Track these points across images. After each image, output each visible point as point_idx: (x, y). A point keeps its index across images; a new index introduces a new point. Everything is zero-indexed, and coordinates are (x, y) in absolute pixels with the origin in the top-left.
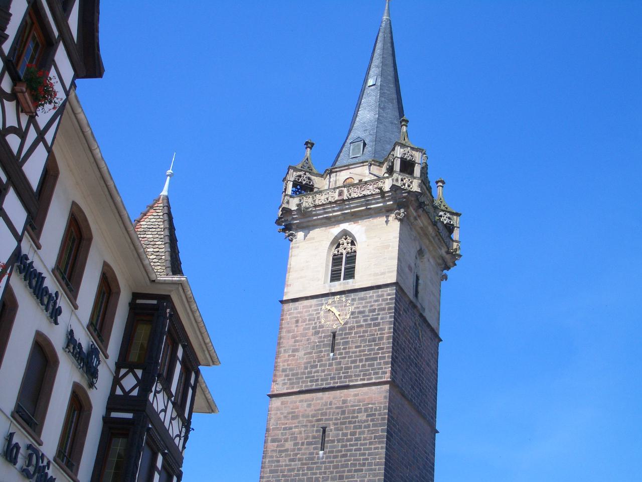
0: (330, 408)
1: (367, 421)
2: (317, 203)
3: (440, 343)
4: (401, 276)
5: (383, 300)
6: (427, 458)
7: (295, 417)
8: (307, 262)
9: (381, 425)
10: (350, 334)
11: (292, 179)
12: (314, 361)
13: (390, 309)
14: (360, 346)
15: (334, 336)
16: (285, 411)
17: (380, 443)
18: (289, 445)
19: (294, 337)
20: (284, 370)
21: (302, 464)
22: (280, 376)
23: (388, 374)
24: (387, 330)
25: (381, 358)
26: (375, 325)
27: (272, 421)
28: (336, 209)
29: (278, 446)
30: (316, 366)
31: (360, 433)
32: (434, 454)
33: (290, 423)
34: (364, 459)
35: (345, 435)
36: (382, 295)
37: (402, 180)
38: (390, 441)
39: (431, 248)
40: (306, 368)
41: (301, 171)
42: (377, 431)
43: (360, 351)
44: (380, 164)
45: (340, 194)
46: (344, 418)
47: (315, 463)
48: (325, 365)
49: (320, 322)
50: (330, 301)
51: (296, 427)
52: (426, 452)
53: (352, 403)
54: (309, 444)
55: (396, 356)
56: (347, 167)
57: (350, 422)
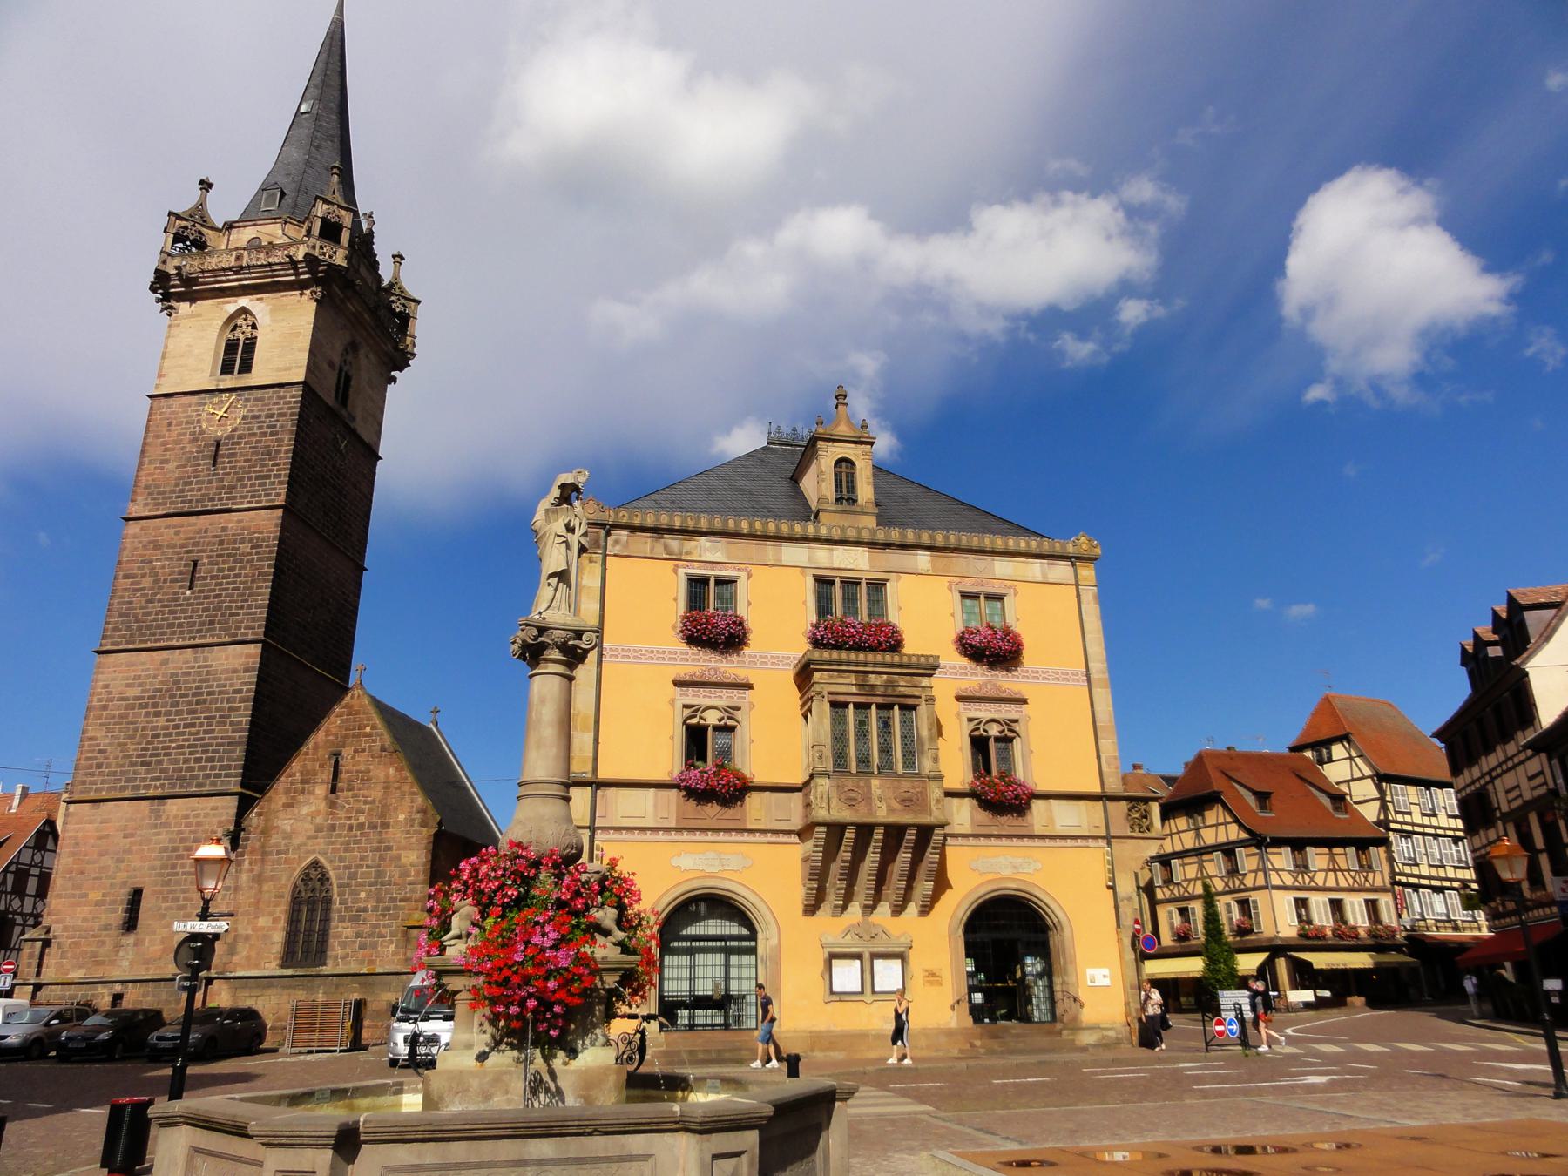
0: (205, 537)
1: (251, 554)
2: (206, 267)
3: (379, 462)
4: (313, 373)
5: (285, 403)
8: (190, 346)
9: (268, 559)
10: (239, 443)
11: (174, 231)
12: (189, 477)
13: (292, 414)
14: (250, 460)
15: (218, 445)
16: (145, 540)
17: (265, 581)
18: (147, 583)
19: (163, 444)
20: (147, 487)
21: (163, 606)
22: (142, 494)
23: (283, 497)
24: (287, 442)
26: (272, 434)
28: (231, 277)
29: (132, 584)
30: (191, 483)
31: (241, 568)
32: (358, 596)
33: (150, 554)
34: (242, 601)
35: (222, 570)
36: (285, 397)
37: (321, 248)
40: (177, 485)
41: (187, 220)
42: (262, 567)
43: (250, 467)
44: (300, 224)
45: (238, 258)
46: (221, 550)
47: (179, 605)
48: (203, 482)
49: (201, 427)
50: (216, 400)
51: (158, 560)
52: (344, 593)
53: (234, 532)
54: (173, 581)
55: (298, 476)
57: (229, 555)
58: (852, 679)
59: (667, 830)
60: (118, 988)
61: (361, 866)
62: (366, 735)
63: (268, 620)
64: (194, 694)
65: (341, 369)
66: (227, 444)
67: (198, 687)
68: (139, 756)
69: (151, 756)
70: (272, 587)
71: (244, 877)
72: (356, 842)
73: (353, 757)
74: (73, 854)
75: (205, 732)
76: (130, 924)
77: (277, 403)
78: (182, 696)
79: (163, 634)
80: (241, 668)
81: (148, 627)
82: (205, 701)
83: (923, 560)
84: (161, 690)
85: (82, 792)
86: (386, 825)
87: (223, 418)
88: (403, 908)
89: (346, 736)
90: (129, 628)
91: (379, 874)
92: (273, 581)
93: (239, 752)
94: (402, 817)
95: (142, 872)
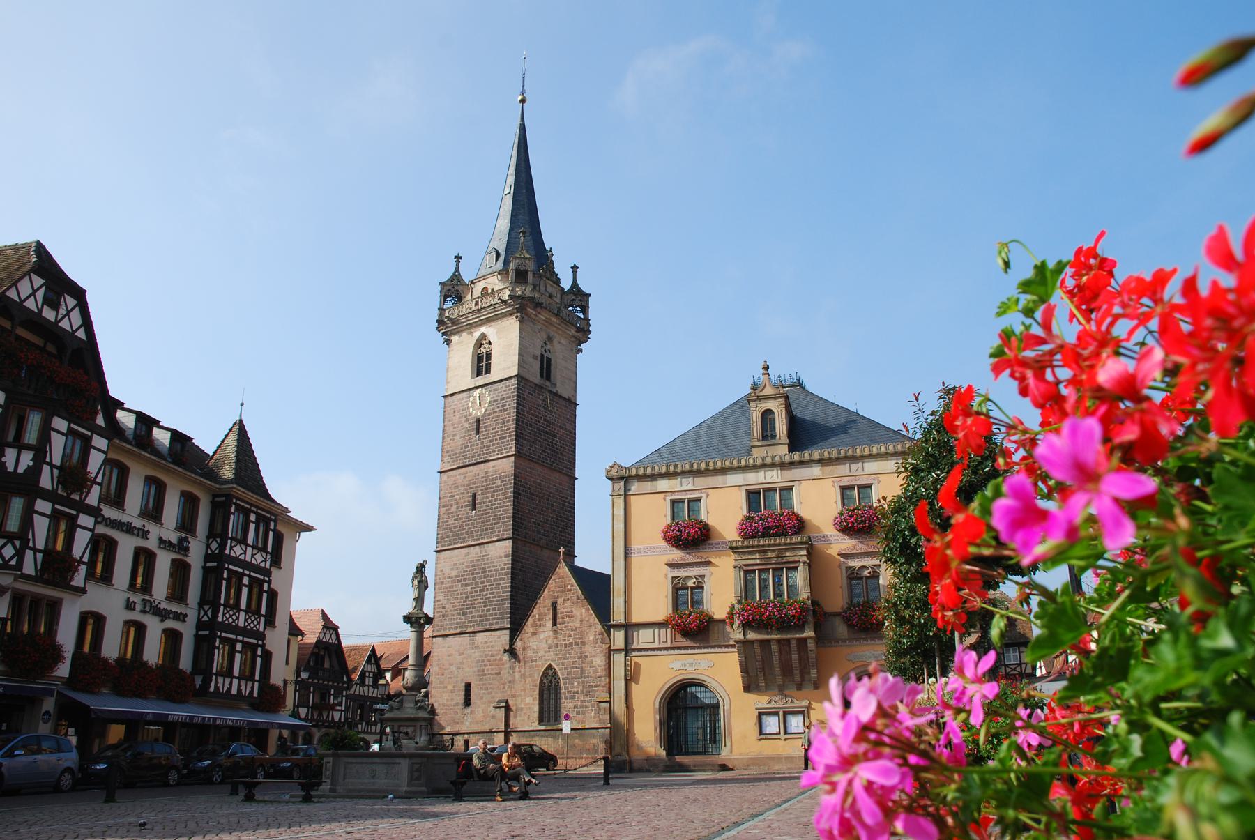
2: (461, 314)
6: (565, 501)
7: (456, 487)
9: (510, 488)
13: (513, 396)
16: (450, 483)
17: (510, 501)
20: (448, 452)
23: (514, 449)
24: (512, 412)
25: (510, 436)
26: (505, 410)
27: (442, 492)
33: (455, 492)
35: (488, 497)
38: (518, 498)
39: (560, 332)
40: (462, 448)
45: (477, 304)
48: (473, 445)
52: (563, 497)
54: (466, 506)
56: (483, 277)
57: (491, 488)
58: (757, 556)
59: (666, 649)
60: (466, 736)
61: (573, 668)
62: (570, 590)
63: (514, 525)
64: (483, 572)
65: (542, 355)
66: (483, 420)
67: (484, 568)
68: (461, 609)
69: (467, 608)
70: (514, 505)
71: (517, 675)
72: (569, 654)
73: (563, 604)
74: (438, 665)
75: (490, 594)
76: (467, 703)
77: (505, 391)
78: (477, 573)
79: (465, 538)
80: (503, 555)
81: (457, 535)
82: (488, 576)
83: (816, 471)
84: (466, 571)
85: (438, 631)
86: (583, 643)
87: (478, 405)
88: (596, 691)
89: (558, 592)
90: (448, 536)
91: (583, 672)
92: (514, 501)
93: (507, 605)
94: (591, 638)
95: (469, 674)
